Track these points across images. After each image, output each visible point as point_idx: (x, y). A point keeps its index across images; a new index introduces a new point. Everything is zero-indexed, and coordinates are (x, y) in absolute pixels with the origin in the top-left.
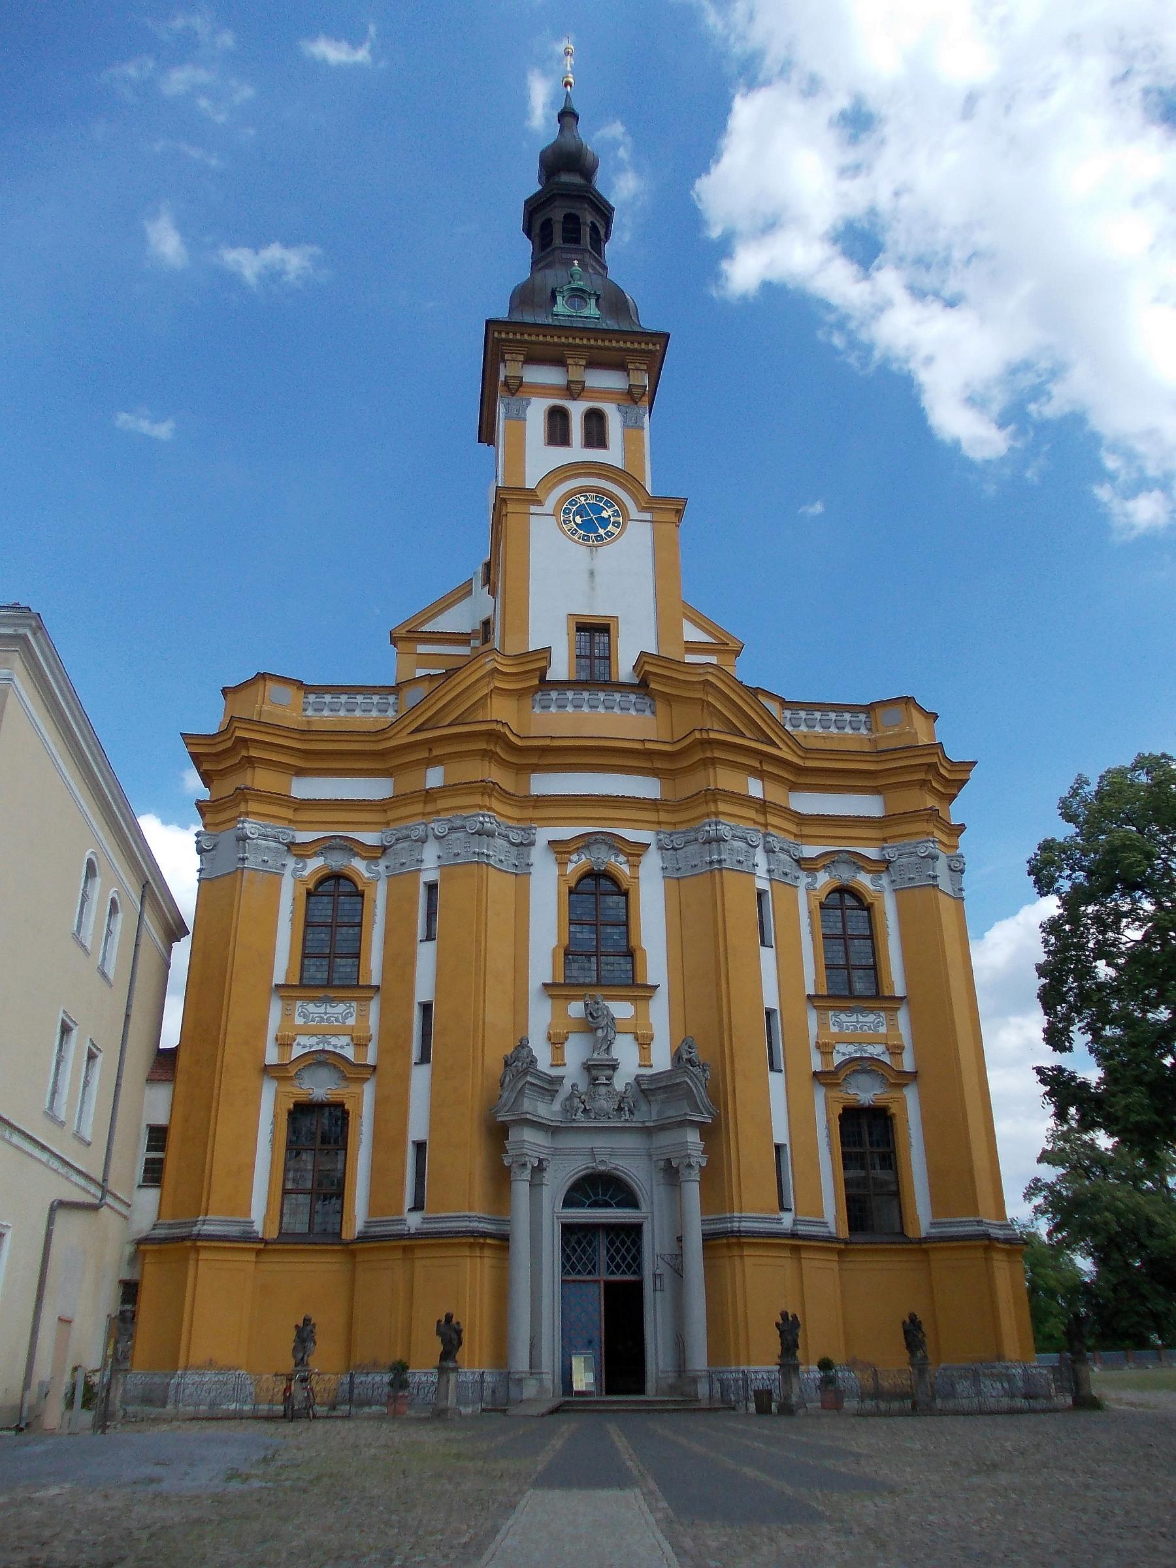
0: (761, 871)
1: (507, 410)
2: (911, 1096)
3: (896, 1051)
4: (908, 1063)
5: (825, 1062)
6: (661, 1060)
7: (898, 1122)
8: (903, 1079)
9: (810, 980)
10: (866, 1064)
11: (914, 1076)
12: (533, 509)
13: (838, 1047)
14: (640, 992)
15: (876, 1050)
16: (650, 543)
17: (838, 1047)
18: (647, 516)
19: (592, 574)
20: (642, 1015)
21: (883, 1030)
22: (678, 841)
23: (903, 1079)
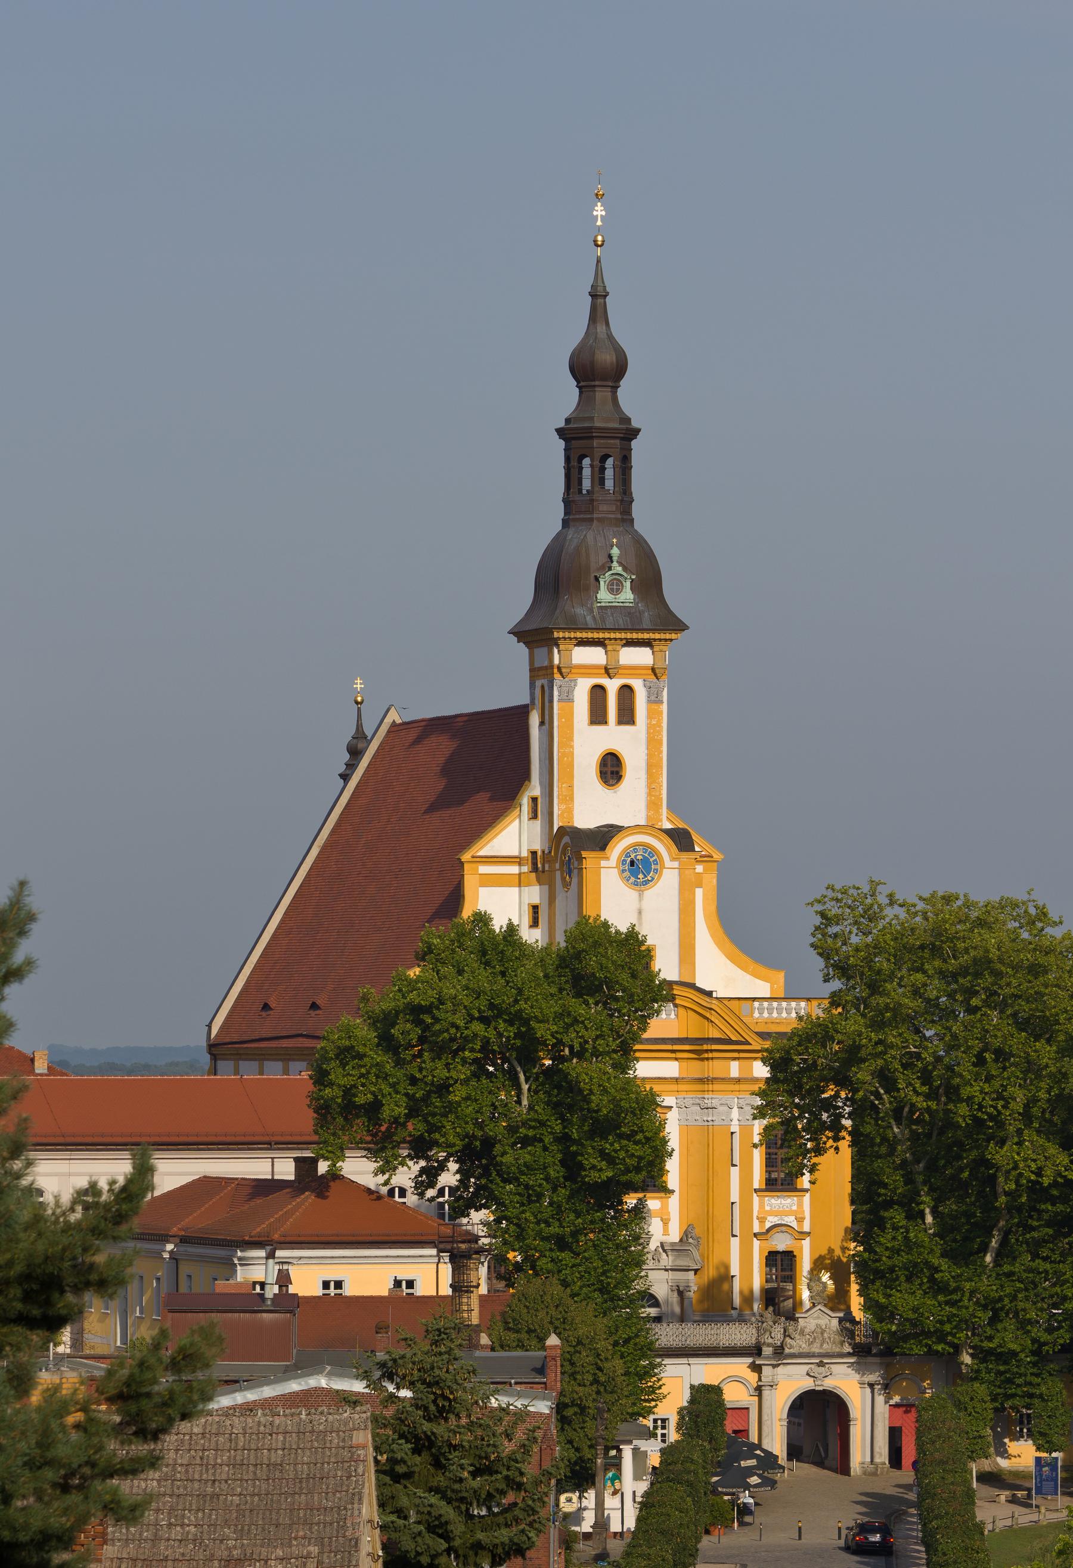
0: (735, 1122)
1: (560, 692)
2: (806, 1243)
3: (800, 1220)
4: (806, 1228)
5: (761, 1227)
6: (674, 1236)
7: (797, 1259)
8: (803, 1235)
9: (758, 1178)
10: (784, 1229)
11: (809, 1234)
12: (603, 863)
13: (769, 1218)
14: (665, 1190)
15: (790, 1220)
16: (677, 886)
17: (769, 1218)
18: (676, 864)
19: (640, 913)
20: (665, 1207)
21: (795, 1208)
22: (689, 1102)
23: (803, 1235)
